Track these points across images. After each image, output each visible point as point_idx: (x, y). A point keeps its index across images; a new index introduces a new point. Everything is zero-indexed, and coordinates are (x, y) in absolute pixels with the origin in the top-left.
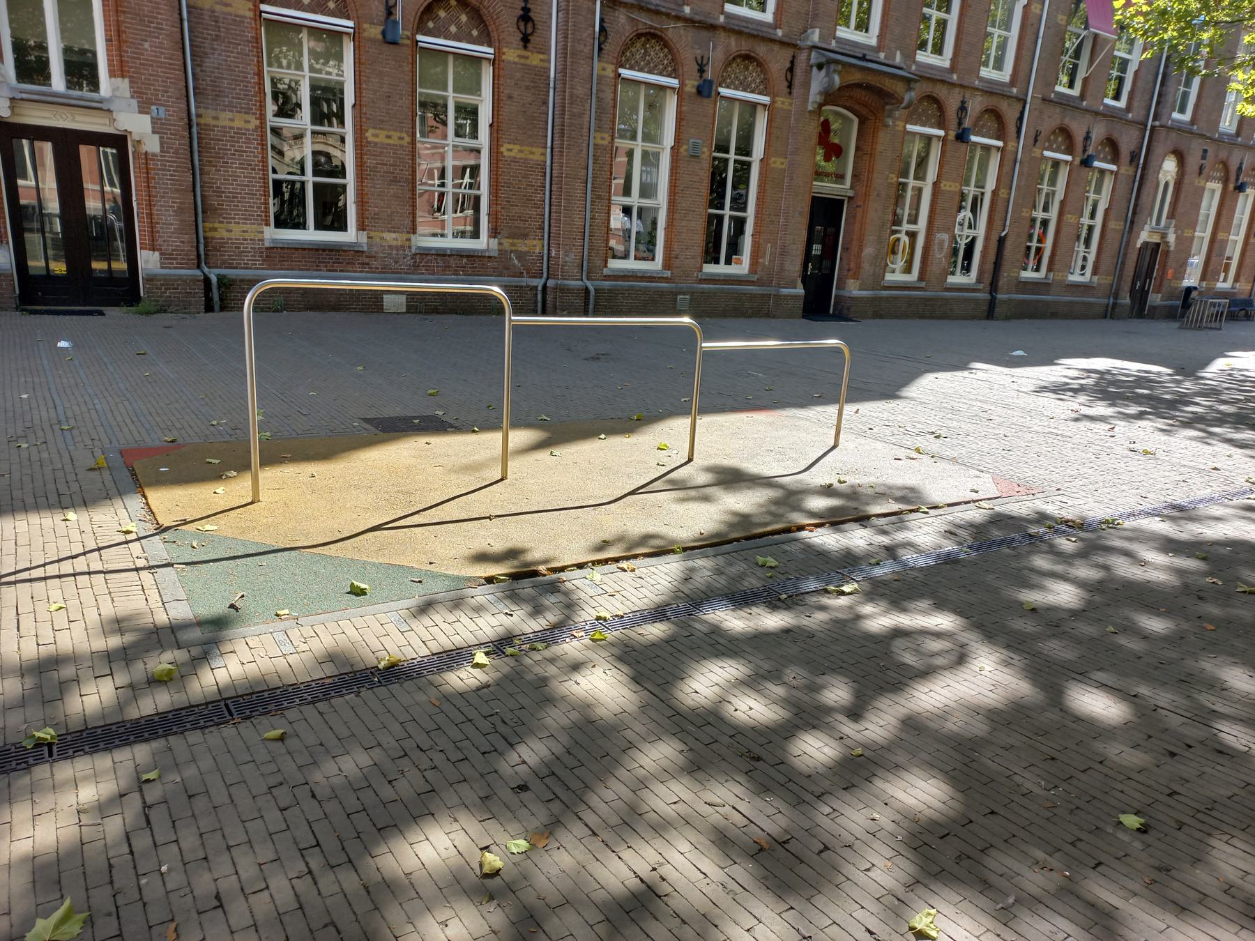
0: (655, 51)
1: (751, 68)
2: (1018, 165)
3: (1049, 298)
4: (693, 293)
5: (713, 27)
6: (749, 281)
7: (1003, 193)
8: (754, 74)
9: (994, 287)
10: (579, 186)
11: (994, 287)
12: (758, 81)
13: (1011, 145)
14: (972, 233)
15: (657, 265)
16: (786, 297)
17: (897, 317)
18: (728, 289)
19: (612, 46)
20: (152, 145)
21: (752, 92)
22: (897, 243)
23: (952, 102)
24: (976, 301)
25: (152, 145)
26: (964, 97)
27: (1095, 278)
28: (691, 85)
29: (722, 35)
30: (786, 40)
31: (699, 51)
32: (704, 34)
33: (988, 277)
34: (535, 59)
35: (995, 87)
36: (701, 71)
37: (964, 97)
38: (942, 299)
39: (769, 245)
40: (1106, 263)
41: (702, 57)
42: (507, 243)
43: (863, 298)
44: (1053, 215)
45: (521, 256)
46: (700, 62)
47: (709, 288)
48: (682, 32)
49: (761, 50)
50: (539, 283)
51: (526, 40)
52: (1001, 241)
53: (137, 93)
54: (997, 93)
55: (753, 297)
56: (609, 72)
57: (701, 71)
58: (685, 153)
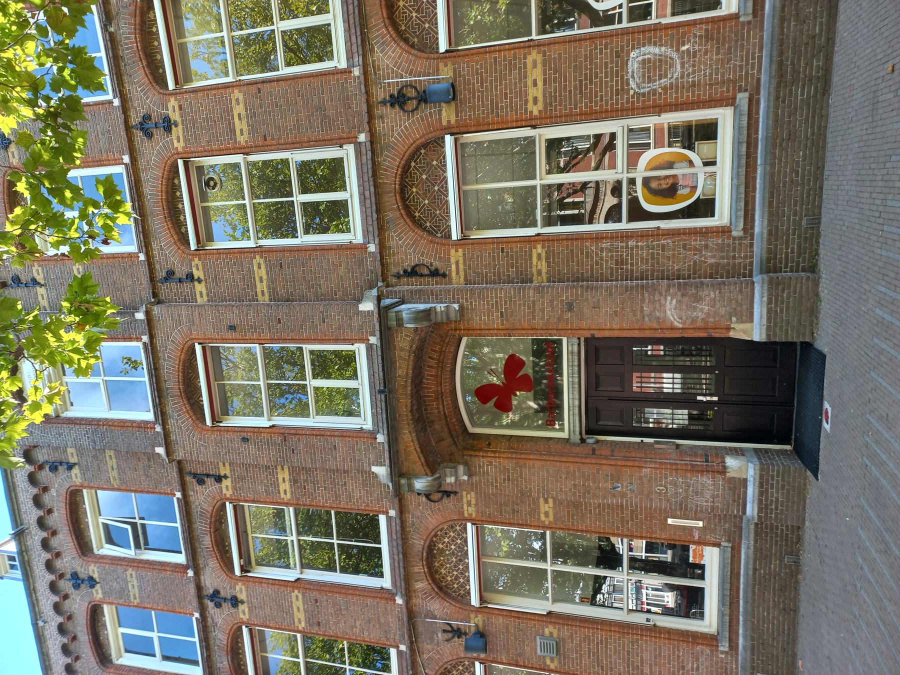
1: (441, 546)
4: (753, 668)
6: (733, 557)
8: (446, 540)
12: (452, 534)
16: (763, 507)
17: (820, 168)
18: (746, 602)
21: (466, 541)
22: (654, 185)
26: (384, 103)
29: (417, 601)
30: (397, 506)
31: (440, 635)
32: (421, 628)
35: (352, 21)
36: (458, 632)
37: (384, 103)
38: (782, 19)
39: (670, 521)
41: (444, 631)
43: (769, 311)
46: (450, 635)
47: (745, 637)
48: (426, 656)
49: (418, 543)
55: (760, 555)
58: (556, 661)
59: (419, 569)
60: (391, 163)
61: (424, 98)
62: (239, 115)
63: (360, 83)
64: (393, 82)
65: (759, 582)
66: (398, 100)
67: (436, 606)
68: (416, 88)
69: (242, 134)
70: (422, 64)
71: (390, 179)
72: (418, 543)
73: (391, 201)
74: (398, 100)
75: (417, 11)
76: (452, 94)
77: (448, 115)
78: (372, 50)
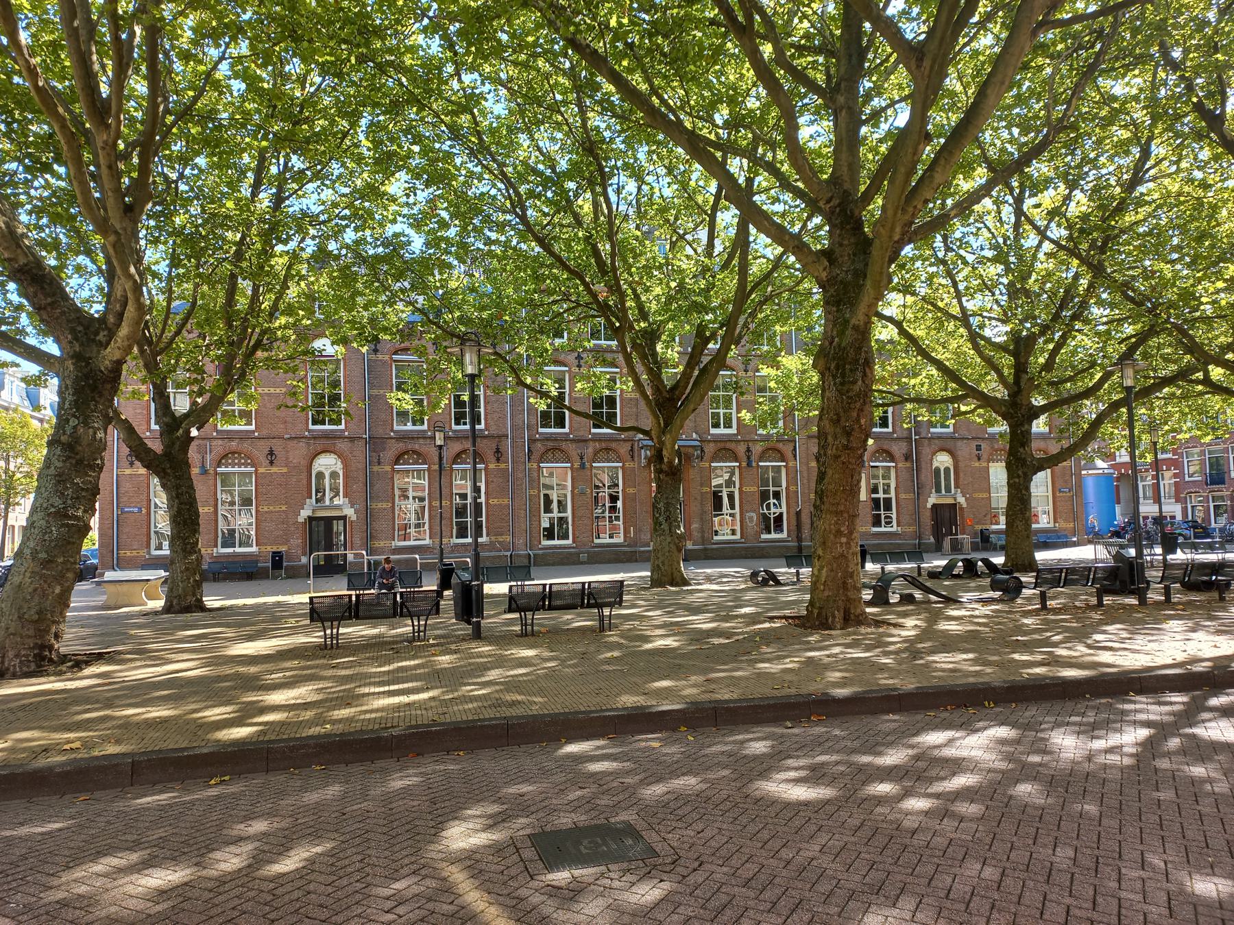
0: (558, 454)
5: (586, 441)
7: (792, 488)
9: (799, 539)
10: (523, 512)
11: (799, 539)
13: (791, 464)
14: (778, 511)
15: (569, 542)
19: (535, 456)
20: (354, 518)
23: (741, 449)
24: (787, 548)
25: (354, 518)
28: (576, 465)
32: (581, 444)
33: (794, 534)
34: (503, 466)
36: (582, 458)
40: (906, 518)
42: (493, 538)
44: (893, 495)
45: (500, 543)
49: (614, 445)
50: (508, 554)
51: (498, 460)
52: (798, 514)
53: (350, 502)
55: (625, 553)
56: (535, 465)
57: (582, 458)
59: (604, 445)
60: (732, 446)
61: (749, 458)
64: (752, 449)
65: (617, 553)
66: (748, 450)
67: (590, 450)
71: (728, 445)
72: (614, 445)
73: (722, 445)
74: (748, 450)
76: (749, 465)
77: (744, 464)
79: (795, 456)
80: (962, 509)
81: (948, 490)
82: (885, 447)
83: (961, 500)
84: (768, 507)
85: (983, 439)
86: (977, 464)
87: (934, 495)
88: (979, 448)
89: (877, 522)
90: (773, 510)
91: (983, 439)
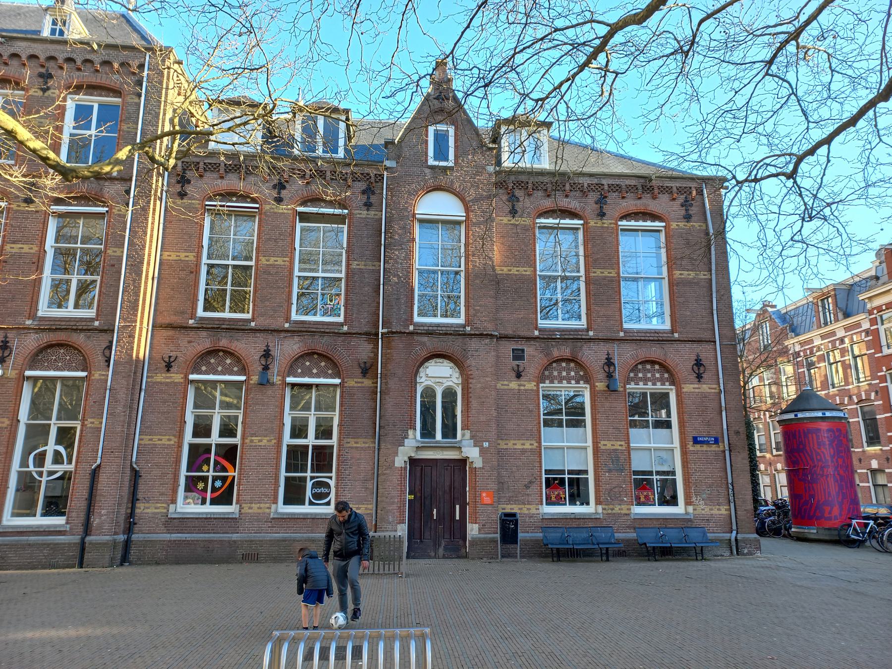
2: (108, 392)
3: (235, 537)
13: (96, 375)
14: (61, 468)
24: (55, 547)
27: (690, 509)
37: (6, 337)
54: (60, 329)
62: (23, 248)
63: (21, 324)
68: (8, 356)
69: (11, 248)
70: (20, 360)
75: (55, 360)
78: (36, 333)
79: (108, 361)
80: (474, 470)
81: (450, 430)
82: (320, 349)
83: (472, 453)
84: (40, 460)
85: (529, 339)
86: (514, 385)
87: (414, 437)
88: (518, 355)
89: (294, 494)
90: (49, 465)
91: (529, 339)
